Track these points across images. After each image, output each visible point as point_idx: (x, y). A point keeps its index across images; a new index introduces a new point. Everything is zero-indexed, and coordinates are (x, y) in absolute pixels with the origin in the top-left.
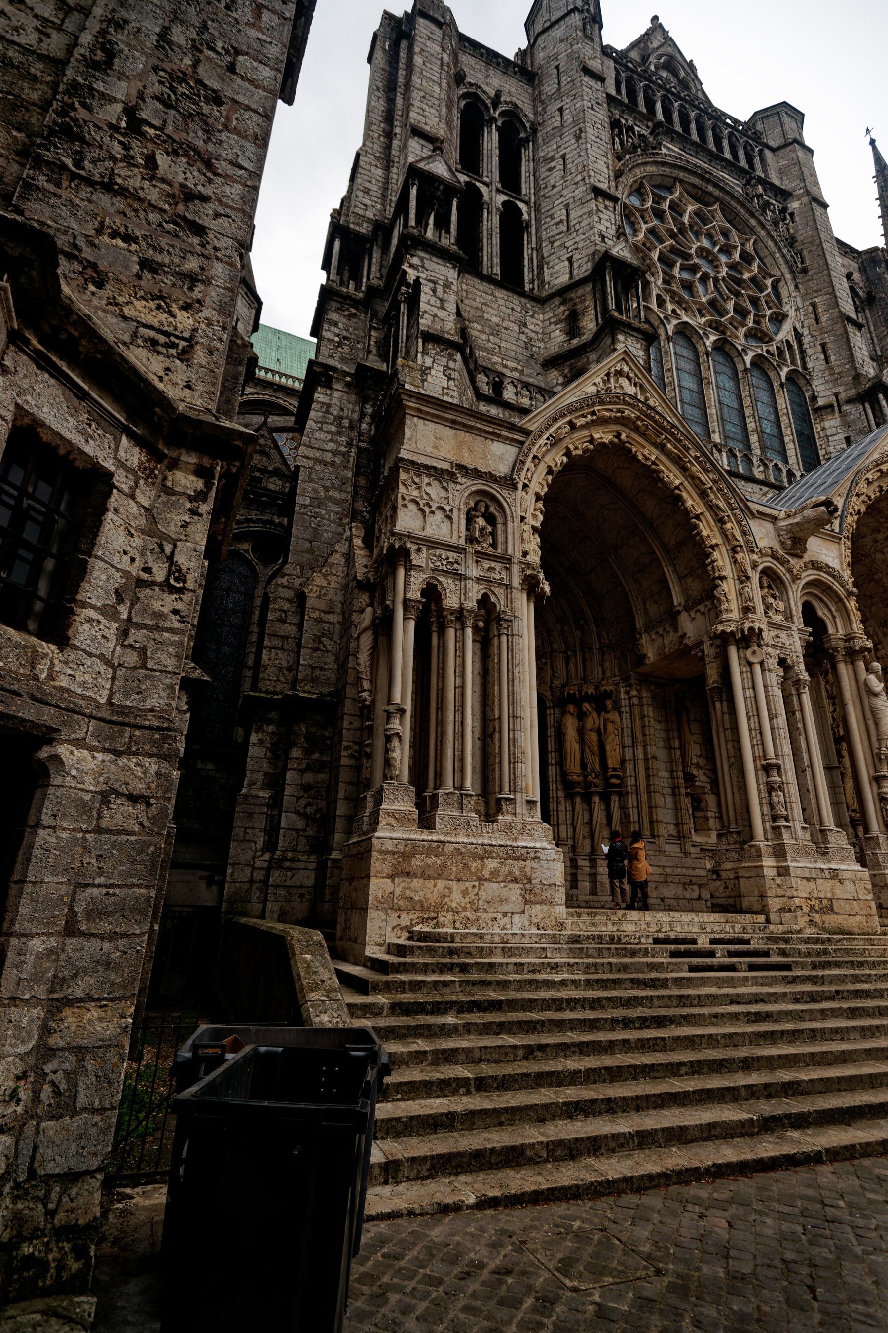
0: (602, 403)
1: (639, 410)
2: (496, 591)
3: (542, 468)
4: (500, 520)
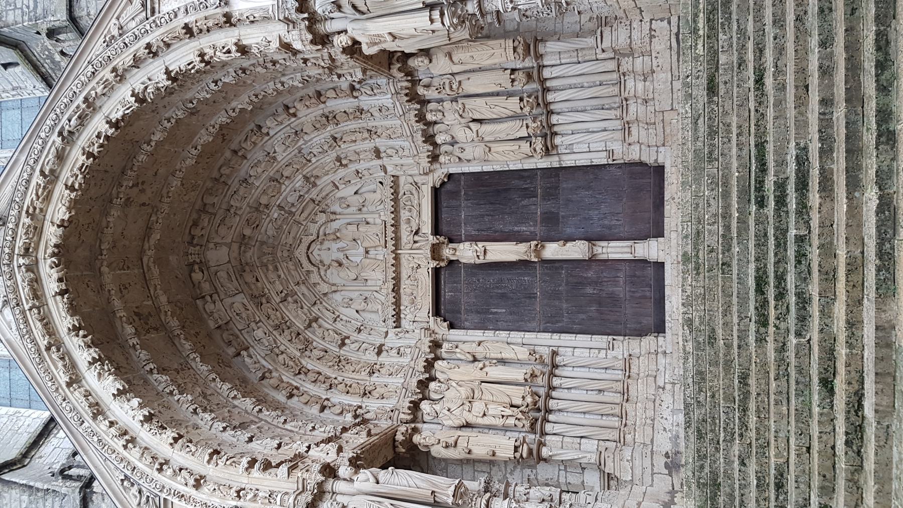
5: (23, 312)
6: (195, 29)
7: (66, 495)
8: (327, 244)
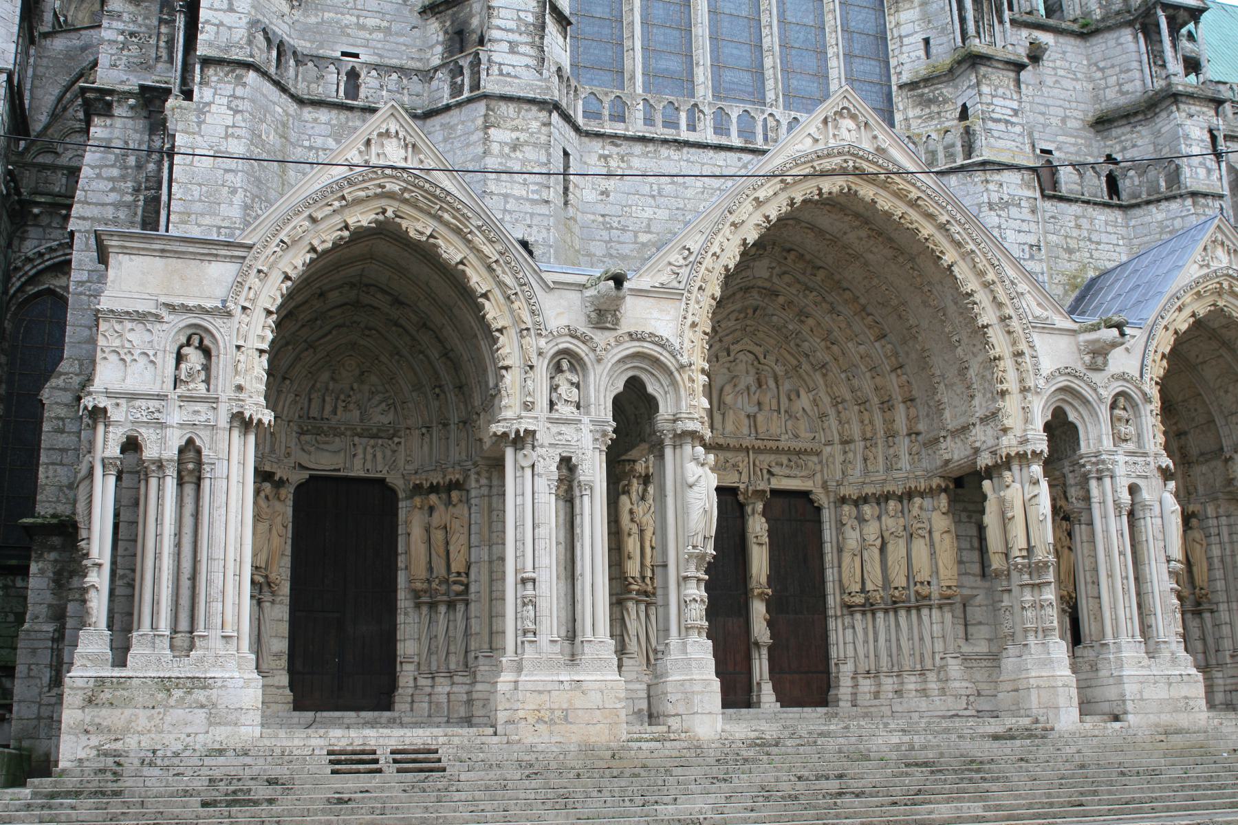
0: (351, 184)
1: (404, 181)
2: (200, 433)
3: (276, 277)
4: (214, 353)
5: (812, 161)
6: (1020, 360)
7: (541, 74)
8: (752, 371)
